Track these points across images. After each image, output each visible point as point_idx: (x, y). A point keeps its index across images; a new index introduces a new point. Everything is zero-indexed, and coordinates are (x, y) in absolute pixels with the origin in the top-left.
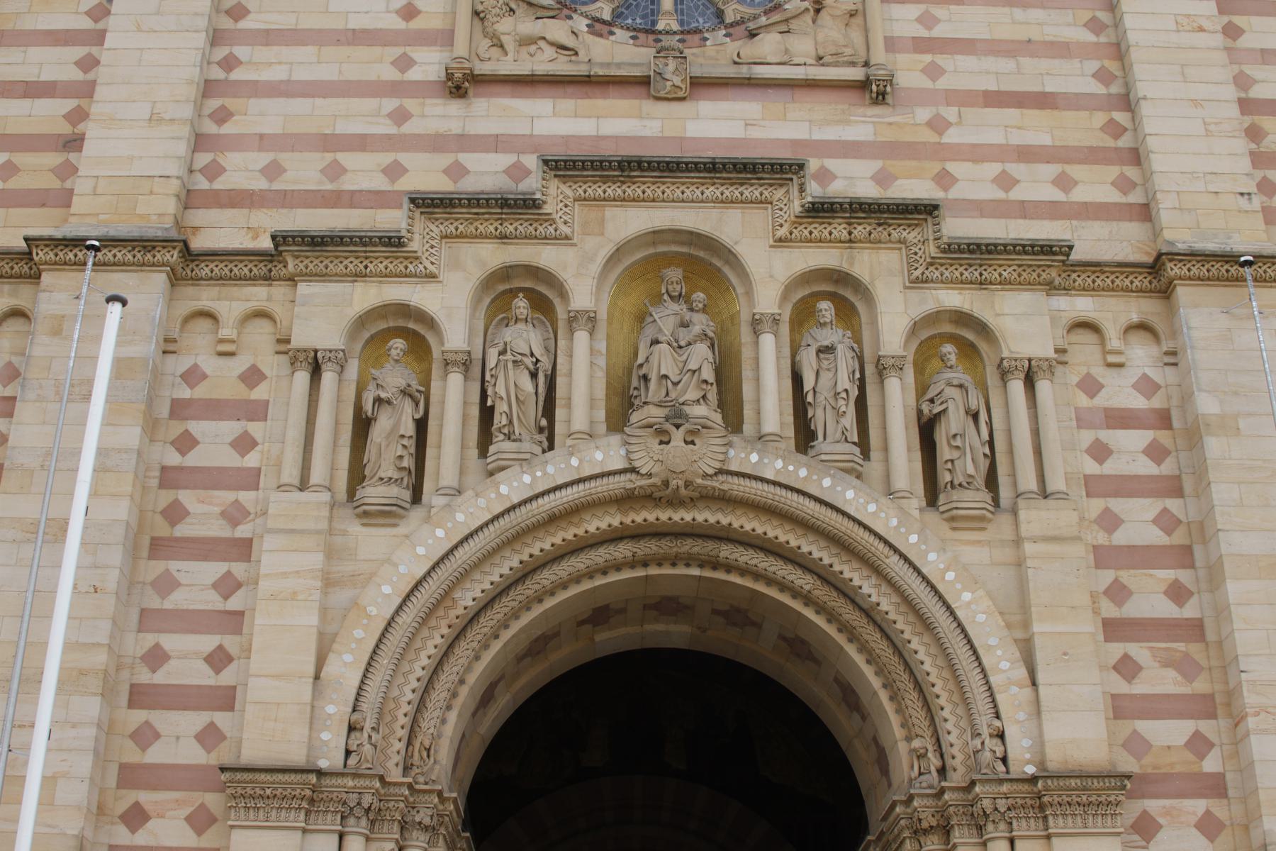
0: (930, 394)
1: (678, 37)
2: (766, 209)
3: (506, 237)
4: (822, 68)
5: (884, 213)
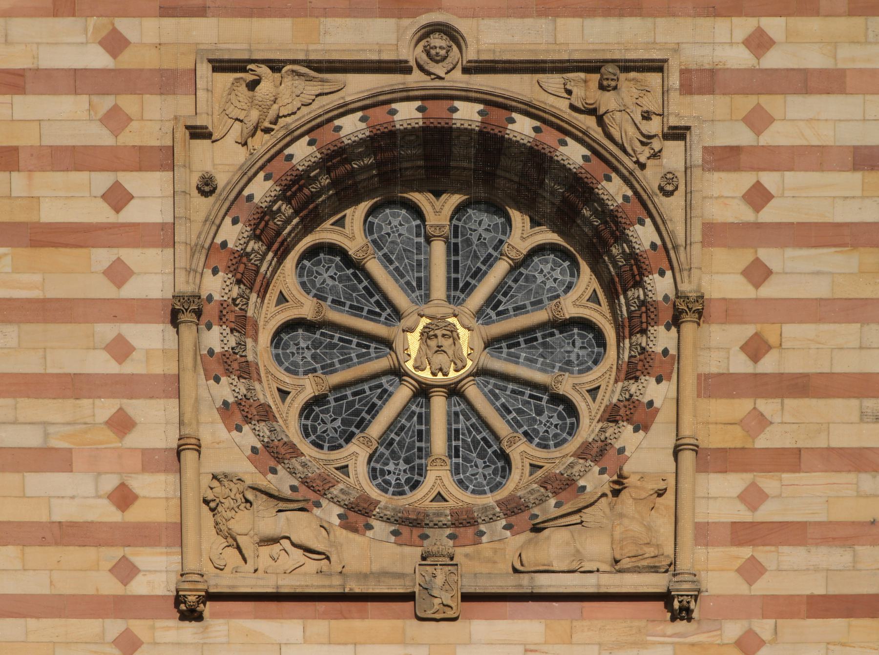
1: (448, 531)
4: (619, 575)
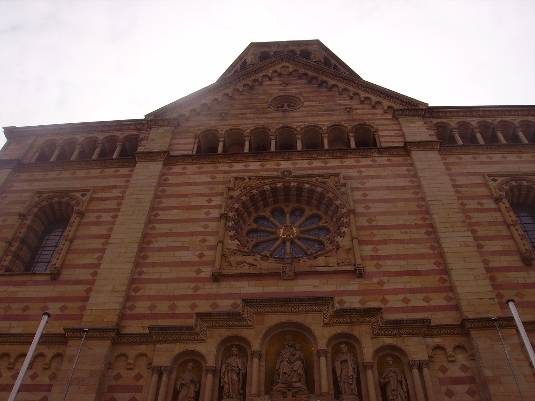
0: (383, 376)
1: (290, 260)
2: (321, 313)
3: (230, 326)
5: (362, 312)
